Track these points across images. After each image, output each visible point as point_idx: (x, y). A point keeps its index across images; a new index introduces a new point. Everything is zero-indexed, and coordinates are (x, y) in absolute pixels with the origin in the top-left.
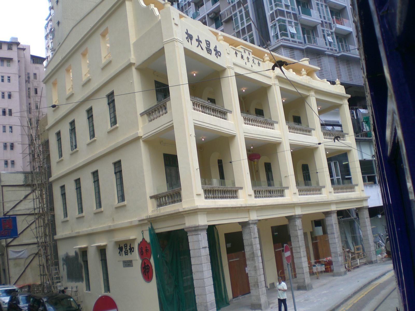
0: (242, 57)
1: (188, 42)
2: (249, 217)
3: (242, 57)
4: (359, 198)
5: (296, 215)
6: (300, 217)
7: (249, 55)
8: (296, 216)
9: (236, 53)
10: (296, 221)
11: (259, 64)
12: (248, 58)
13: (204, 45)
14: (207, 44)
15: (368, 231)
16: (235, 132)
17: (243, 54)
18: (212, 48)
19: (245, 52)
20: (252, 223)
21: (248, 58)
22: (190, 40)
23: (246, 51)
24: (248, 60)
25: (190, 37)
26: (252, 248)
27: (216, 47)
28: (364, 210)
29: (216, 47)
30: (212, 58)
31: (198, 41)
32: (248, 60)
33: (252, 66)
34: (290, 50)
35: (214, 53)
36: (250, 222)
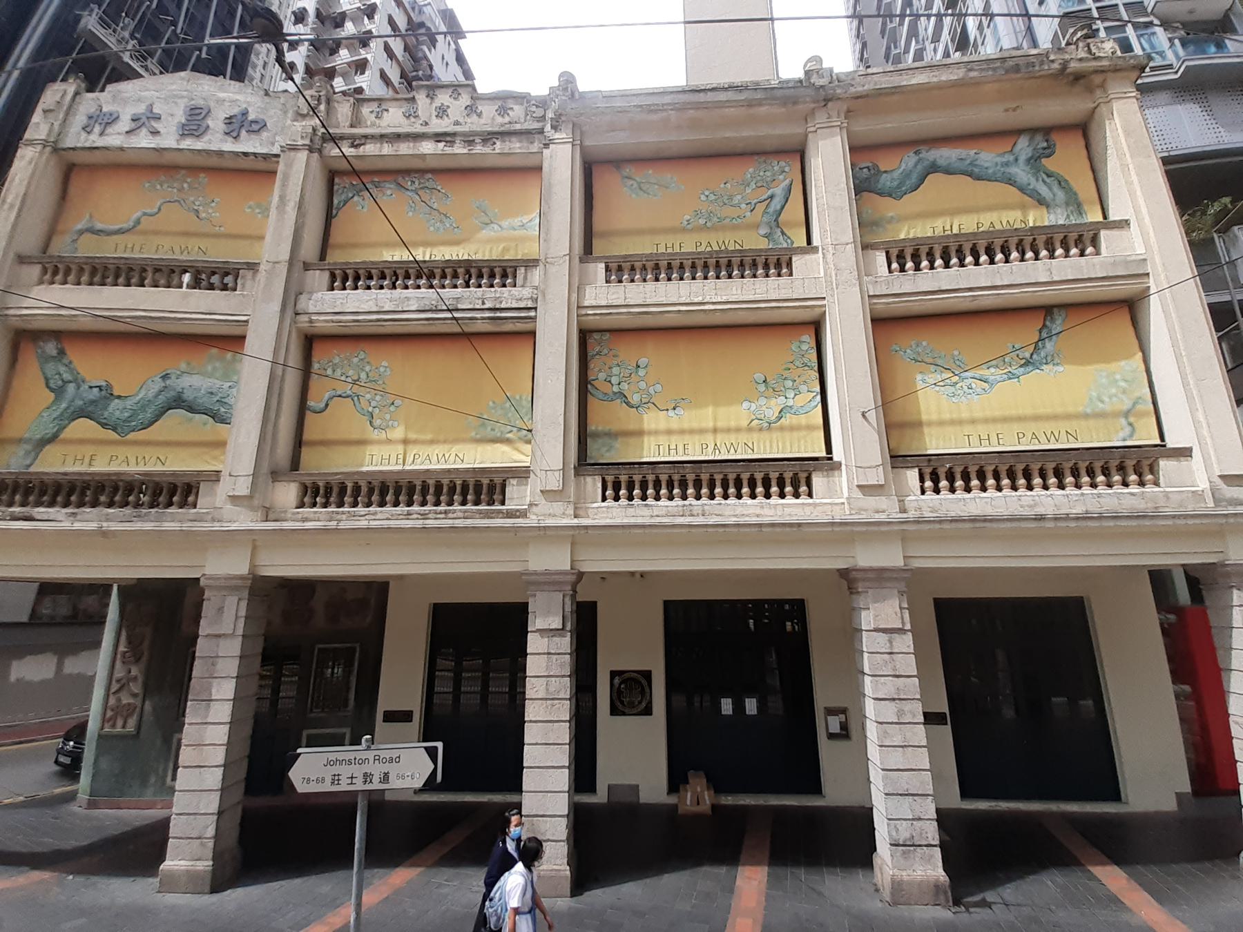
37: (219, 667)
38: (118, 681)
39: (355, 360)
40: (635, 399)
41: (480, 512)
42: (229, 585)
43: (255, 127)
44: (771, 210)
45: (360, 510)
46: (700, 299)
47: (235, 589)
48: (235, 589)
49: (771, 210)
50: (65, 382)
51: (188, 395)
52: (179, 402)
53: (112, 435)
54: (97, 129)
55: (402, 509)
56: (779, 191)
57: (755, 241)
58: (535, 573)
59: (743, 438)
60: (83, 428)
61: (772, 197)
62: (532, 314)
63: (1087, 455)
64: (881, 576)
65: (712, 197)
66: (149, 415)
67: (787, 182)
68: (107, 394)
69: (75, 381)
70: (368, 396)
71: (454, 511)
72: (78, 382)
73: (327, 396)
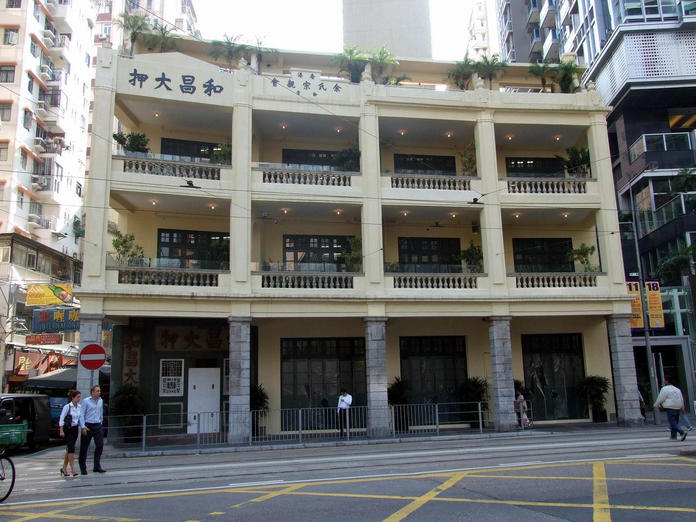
0: (291, 84)
1: (134, 84)
3: (291, 84)
4: (590, 298)
5: (366, 317)
6: (377, 320)
7: (313, 78)
9: (275, 82)
10: (368, 327)
11: (337, 88)
12: (307, 85)
13: (176, 82)
14: (184, 80)
15: (620, 362)
16: (229, 195)
18: (198, 84)
19: (300, 75)
21: (307, 85)
22: (138, 83)
23: (303, 74)
24: (307, 86)
25: (139, 78)
27: (212, 81)
28: (615, 321)
29: (212, 81)
30: (199, 97)
31: (163, 80)
32: (307, 86)
33: (315, 94)
35: (200, 90)
36: (230, 319)
38: (126, 375)
42: (243, 321)
43: (218, 89)
47: (244, 322)
48: (244, 322)
54: (138, 83)
58: (372, 317)
64: (500, 319)
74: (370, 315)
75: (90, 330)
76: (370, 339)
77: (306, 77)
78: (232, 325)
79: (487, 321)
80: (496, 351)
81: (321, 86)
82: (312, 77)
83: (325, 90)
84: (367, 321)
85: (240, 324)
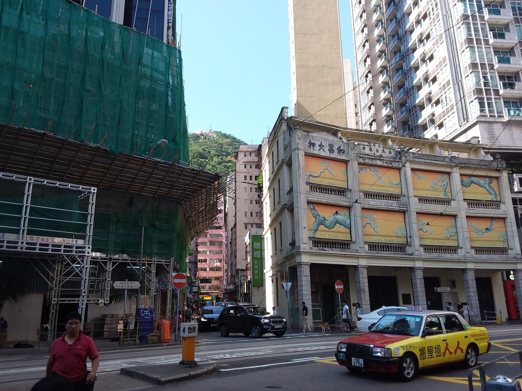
0: (371, 150)
2: (358, 263)
3: (371, 150)
8: (416, 268)
17: (373, 147)
19: (374, 145)
20: (360, 267)
23: (376, 144)
26: (360, 285)
34: (488, 124)
36: (359, 266)
37: (365, 284)
39: (369, 215)
40: (424, 230)
41: (403, 254)
42: (364, 267)
44: (444, 188)
45: (382, 252)
46: (437, 210)
49: (444, 188)
50: (316, 216)
51: (339, 220)
52: (337, 222)
53: (327, 229)
55: (388, 252)
56: (445, 183)
57: (441, 196)
59: (443, 241)
60: (322, 227)
61: (444, 185)
62: (406, 209)
63: (494, 249)
65: (433, 183)
66: (333, 225)
67: (447, 182)
68: (325, 219)
69: (318, 215)
70: (373, 224)
71: (399, 253)
72: (319, 216)
73: (365, 223)
74: (416, 266)
75: (306, 270)
76: (417, 278)
77: (377, 145)
78: (360, 269)
79: (464, 271)
80: (470, 286)
81: (383, 151)
82: (379, 146)
83: (385, 153)
84: (415, 269)
85: (363, 268)
